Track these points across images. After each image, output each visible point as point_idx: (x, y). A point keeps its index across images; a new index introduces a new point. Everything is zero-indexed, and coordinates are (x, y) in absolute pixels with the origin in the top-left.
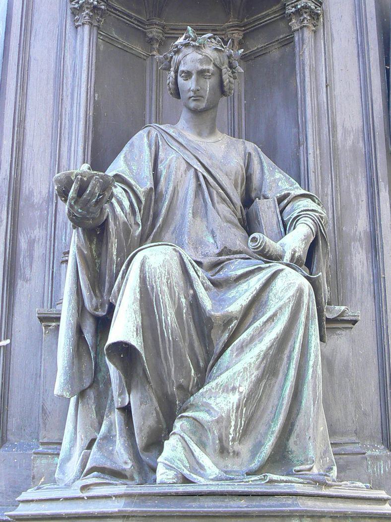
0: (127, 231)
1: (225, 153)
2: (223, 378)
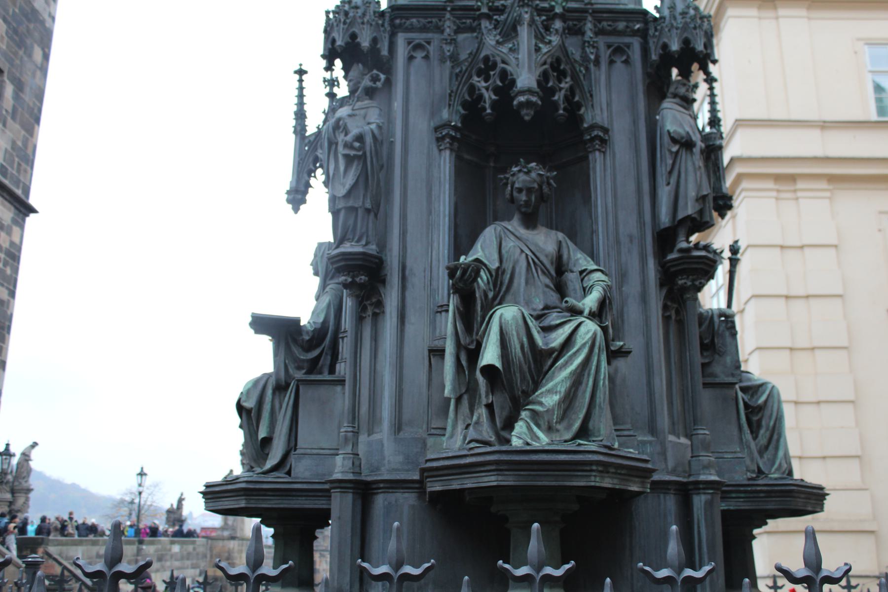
0: (486, 295)
1: (545, 241)
2: (550, 385)
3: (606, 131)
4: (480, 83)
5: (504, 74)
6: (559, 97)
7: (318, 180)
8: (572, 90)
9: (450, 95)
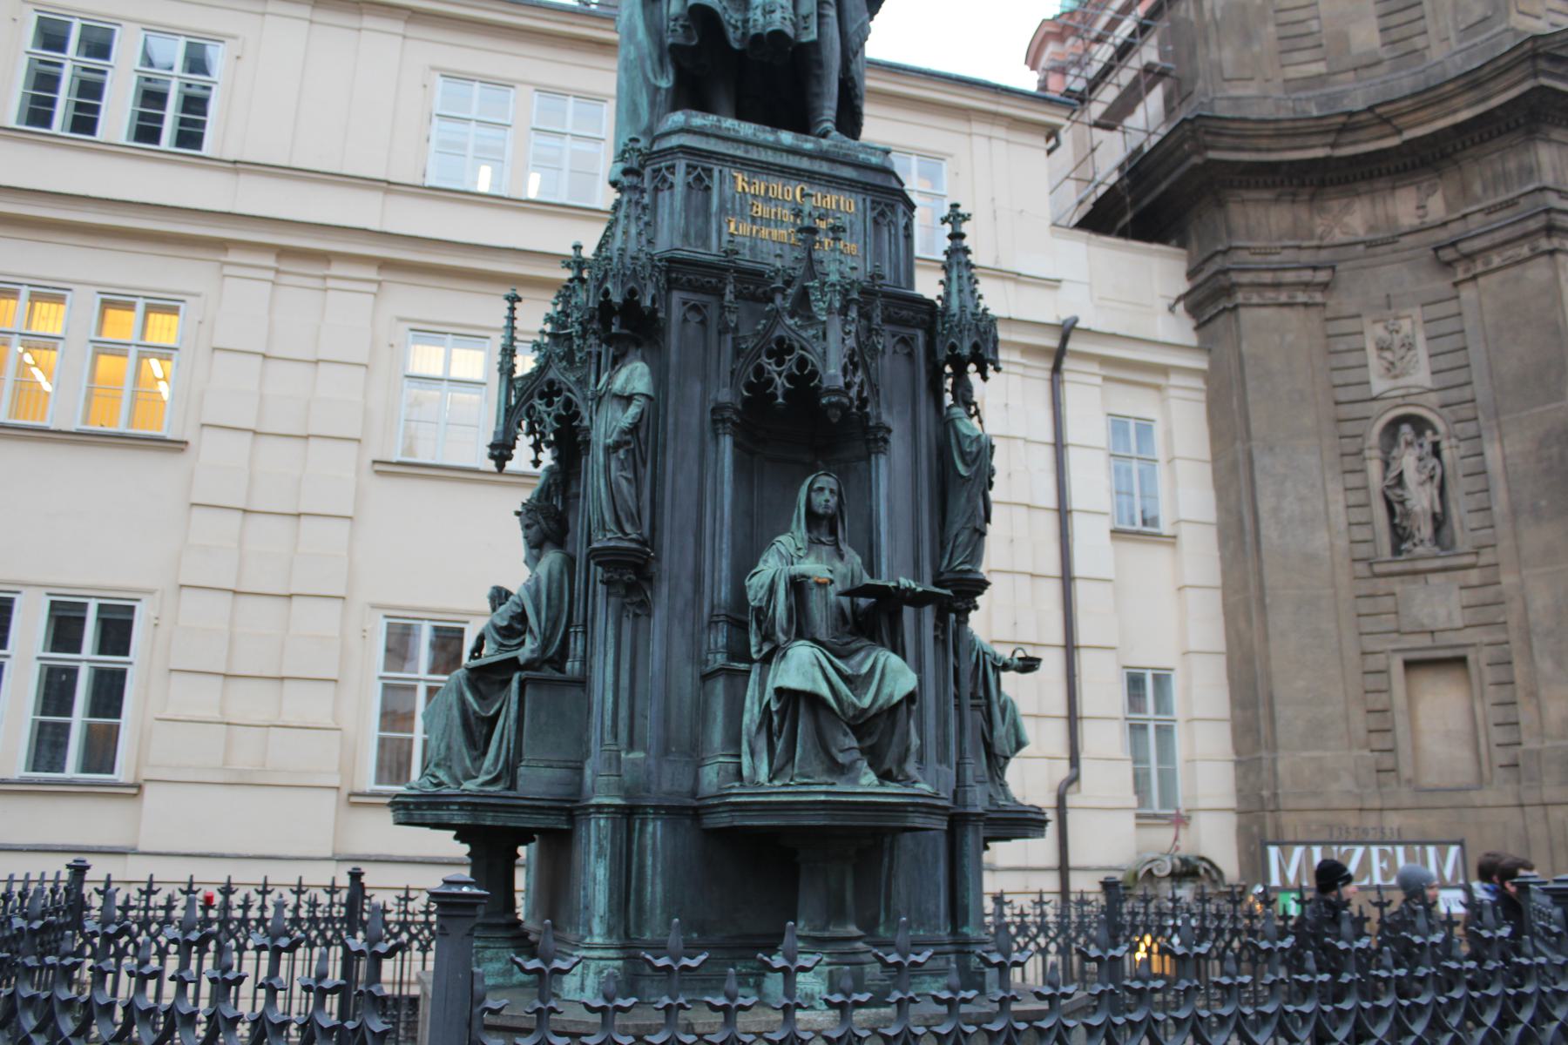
3: (889, 431)
4: (770, 366)
5: (802, 363)
9: (732, 373)
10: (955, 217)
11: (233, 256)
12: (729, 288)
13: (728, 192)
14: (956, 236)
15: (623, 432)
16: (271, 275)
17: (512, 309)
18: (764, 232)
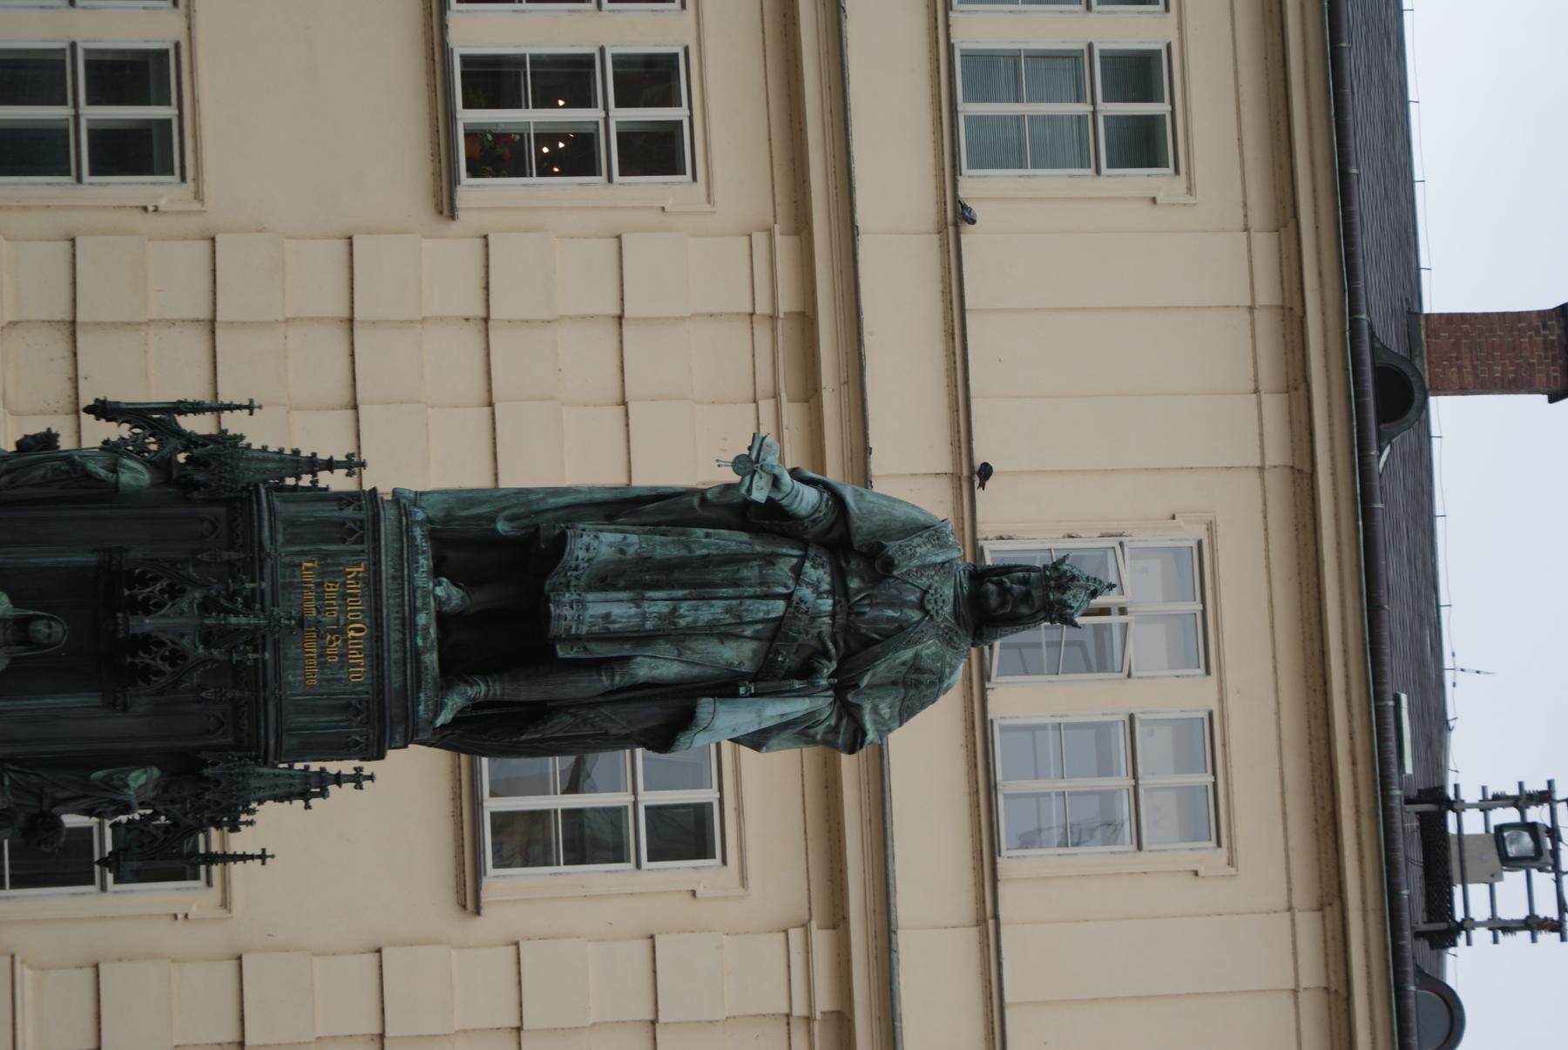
3: (125, 708)
4: (159, 586)
5: (160, 606)
6: (144, 658)
7: (117, 431)
8: (159, 673)
10: (358, 779)
11: (785, 245)
12: (233, 555)
13: (343, 560)
14: (338, 779)
15: (83, 465)
16: (763, 308)
17: (240, 407)
18: (311, 595)
